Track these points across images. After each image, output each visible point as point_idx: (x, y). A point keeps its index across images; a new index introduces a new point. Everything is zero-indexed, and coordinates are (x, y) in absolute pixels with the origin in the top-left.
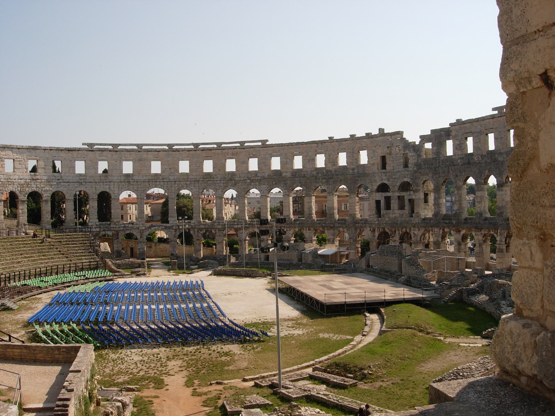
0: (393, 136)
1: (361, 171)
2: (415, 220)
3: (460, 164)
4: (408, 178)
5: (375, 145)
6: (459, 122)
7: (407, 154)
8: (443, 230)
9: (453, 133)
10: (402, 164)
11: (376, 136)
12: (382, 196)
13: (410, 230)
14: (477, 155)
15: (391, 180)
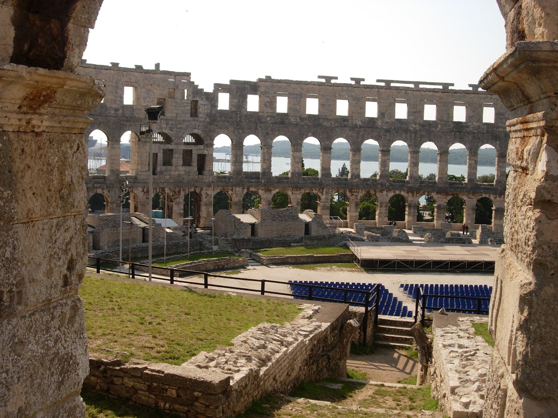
0: (177, 77)
1: (128, 114)
2: (206, 178)
3: (270, 122)
4: (198, 129)
5: (150, 83)
6: (268, 78)
7: (197, 101)
8: (248, 189)
9: (262, 89)
10: (190, 112)
11: (148, 72)
12: (159, 148)
13: (202, 189)
14: (294, 116)
15: (175, 130)
